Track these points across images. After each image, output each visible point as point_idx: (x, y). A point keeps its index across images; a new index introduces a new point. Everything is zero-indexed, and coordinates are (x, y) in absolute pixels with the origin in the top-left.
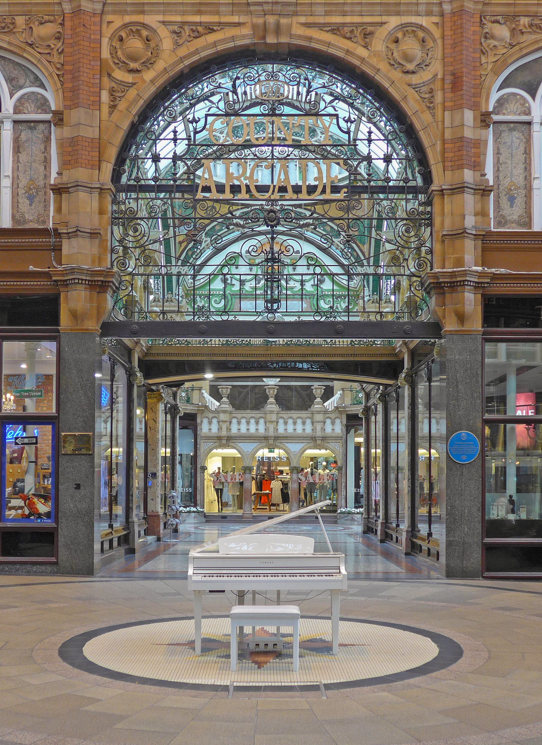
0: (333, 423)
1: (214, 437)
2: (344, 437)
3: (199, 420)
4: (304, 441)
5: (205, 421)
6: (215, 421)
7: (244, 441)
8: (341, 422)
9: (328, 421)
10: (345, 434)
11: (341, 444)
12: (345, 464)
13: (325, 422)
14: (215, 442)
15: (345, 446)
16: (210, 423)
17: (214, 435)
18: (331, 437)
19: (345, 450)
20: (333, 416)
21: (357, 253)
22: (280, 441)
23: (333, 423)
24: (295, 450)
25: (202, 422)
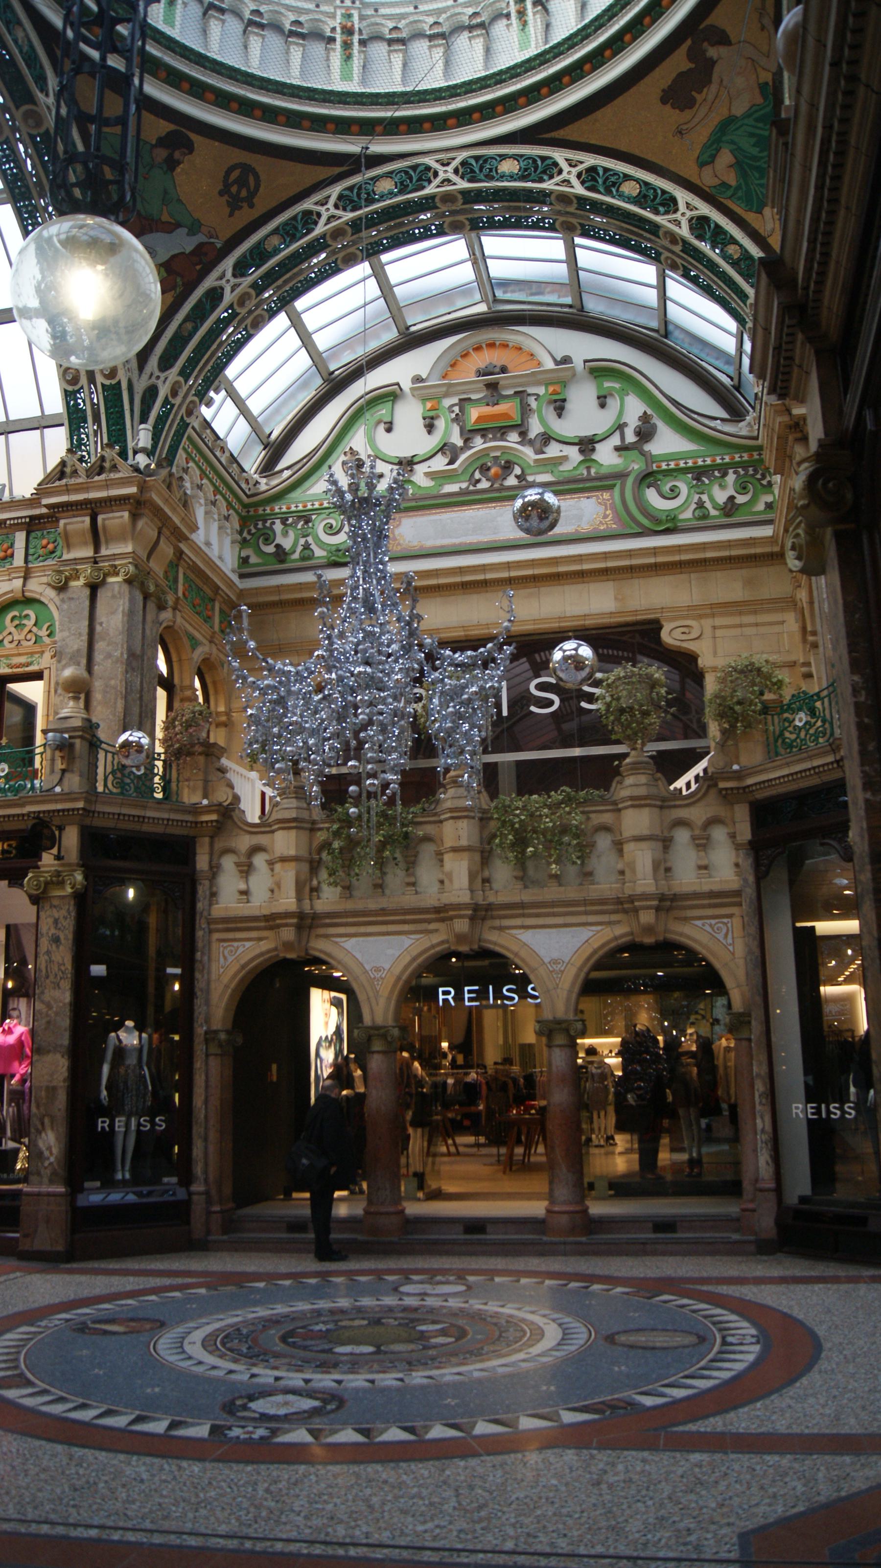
0: (702, 843)
1: (255, 919)
2: (750, 892)
3: (202, 862)
4: (591, 919)
5: (228, 863)
6: (259, 860)
7: (362, 929)
8: (732, 836)
9: (682, 836)
10: (751, 879)
11: (737, 922)
12: (759, 1000)
13: (666, 843)
14: (260, 939)
15: (753, 930)
16: (246, 869)
17: (257, 913)
18: (696, 895)
19: (755, 945)
20: (697, 814)
21: (741, 246)
22: (497, 923)
23: (702, 843)
24: (555, 955)
25: (215, 869)
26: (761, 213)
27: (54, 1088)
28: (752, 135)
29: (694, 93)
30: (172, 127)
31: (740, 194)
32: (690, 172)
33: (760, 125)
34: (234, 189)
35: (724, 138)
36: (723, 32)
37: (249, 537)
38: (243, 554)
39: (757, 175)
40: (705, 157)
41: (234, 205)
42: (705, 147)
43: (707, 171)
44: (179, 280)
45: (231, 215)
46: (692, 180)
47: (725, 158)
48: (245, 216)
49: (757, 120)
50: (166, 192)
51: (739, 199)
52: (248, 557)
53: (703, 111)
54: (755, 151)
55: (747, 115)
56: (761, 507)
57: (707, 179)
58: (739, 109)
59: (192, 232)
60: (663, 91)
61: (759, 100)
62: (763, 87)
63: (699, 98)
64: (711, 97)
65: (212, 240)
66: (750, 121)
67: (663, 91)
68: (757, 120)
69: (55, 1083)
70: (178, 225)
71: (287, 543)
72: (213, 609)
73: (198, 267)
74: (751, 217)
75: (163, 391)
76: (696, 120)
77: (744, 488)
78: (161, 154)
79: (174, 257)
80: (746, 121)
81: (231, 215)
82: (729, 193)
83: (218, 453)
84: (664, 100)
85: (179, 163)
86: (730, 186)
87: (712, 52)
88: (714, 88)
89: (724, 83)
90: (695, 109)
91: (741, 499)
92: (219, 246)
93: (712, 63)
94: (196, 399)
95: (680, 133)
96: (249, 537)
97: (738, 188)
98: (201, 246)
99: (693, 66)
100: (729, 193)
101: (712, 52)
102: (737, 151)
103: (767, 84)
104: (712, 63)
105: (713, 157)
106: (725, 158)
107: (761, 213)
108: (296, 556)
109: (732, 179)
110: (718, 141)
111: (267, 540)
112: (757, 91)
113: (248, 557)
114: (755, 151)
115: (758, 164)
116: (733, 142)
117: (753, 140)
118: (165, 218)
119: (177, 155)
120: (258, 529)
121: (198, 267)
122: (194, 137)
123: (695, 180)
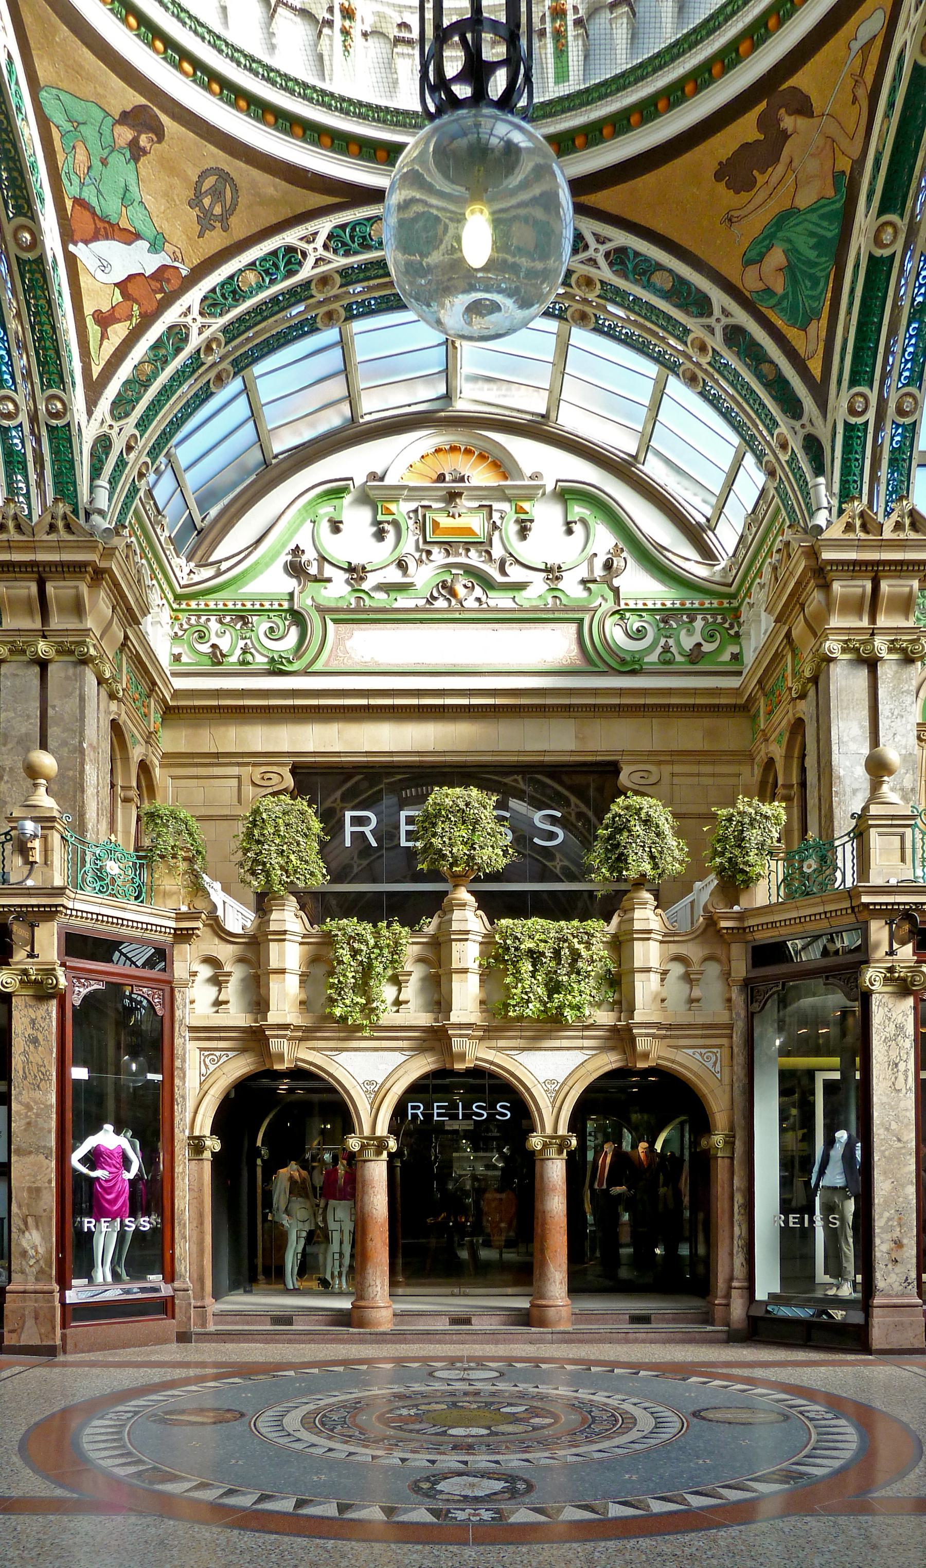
26: (805, 330)
27: (38, 1190)
28: (812, 234)
29: (755, 172)
30: (143, 101)
31: (785, 304)
32: (732, 273)
33: (825, 224)
34: (207, 201)
35: (780, 234)
36: (808, 98)
37: (180, 633)
38: (176, 651)
39: (808, 284)
40: (753, 254)
41: (206, 222)
42: (755, 242)
43: (751, 272)
44: (135, 307)
45: (201, 235)
46: (734, 282)
47: (777, 257)
48: (216, 241)
49: (822, 217)
50: (126, 189)
51: (782, 310)
52: (180, 654)
53: (762, 196)
54: (812, 255)
55: (812, 210)
56: (726, 657)
57: (750, 282)
58: (804, 200)
59: (155, 248)
60: (720, 163)
61: (830, 193)
62: (838, 176)
63: (761, 179)
64: (774, 180)
65: (176, 264)
66: (814, 217)
67: (720, 163)
68: (822, 217)
69: (38, 1184)
70: (138, 236)
71: (224, 644)
72: (149, 706)
73: (159, 296)
74: (792, 334)
75: (118, 445)
76: (751, 207)
77: (712, 636)
78: (125, 134)
79: (130, 277)
80: (808, 216)
81: (201, 235)
82: (773, 301)
83: (159, 531)
84: (718, 176)
85: (145, 152)
86: (775, 294)
87: (788, 122)
88: (780, 168)
89: (794, 164)
90: (753, 192)
91: (707, 647)
92: (184, 273)
93: (785, 136)
94: (148, 460)
95: (730, 220)
96: (180, 633)
97: (785, 296)
98: (163, 268)
99: (762, 137)
100: (773, 301)
101: (788, 122)
102: (792, 251)
103: (843, 172)
104: (785, 136)
105: (761, 257)
106: (777, 257)
107: (805, 330)
108: (234, 659)
109: (779, 287)
110: (772, 236)
111: (201, 638)
112: (830, 180)
113: (180, 654)
114: (812, 255)
115: (812, 271)
116: (789, 241)
117: (813, 241)
118: (124, 224)
119: (143, 140)
120: (192, 626)
121: (159, 296)
122: (164, 118)
123: (735, 280)
